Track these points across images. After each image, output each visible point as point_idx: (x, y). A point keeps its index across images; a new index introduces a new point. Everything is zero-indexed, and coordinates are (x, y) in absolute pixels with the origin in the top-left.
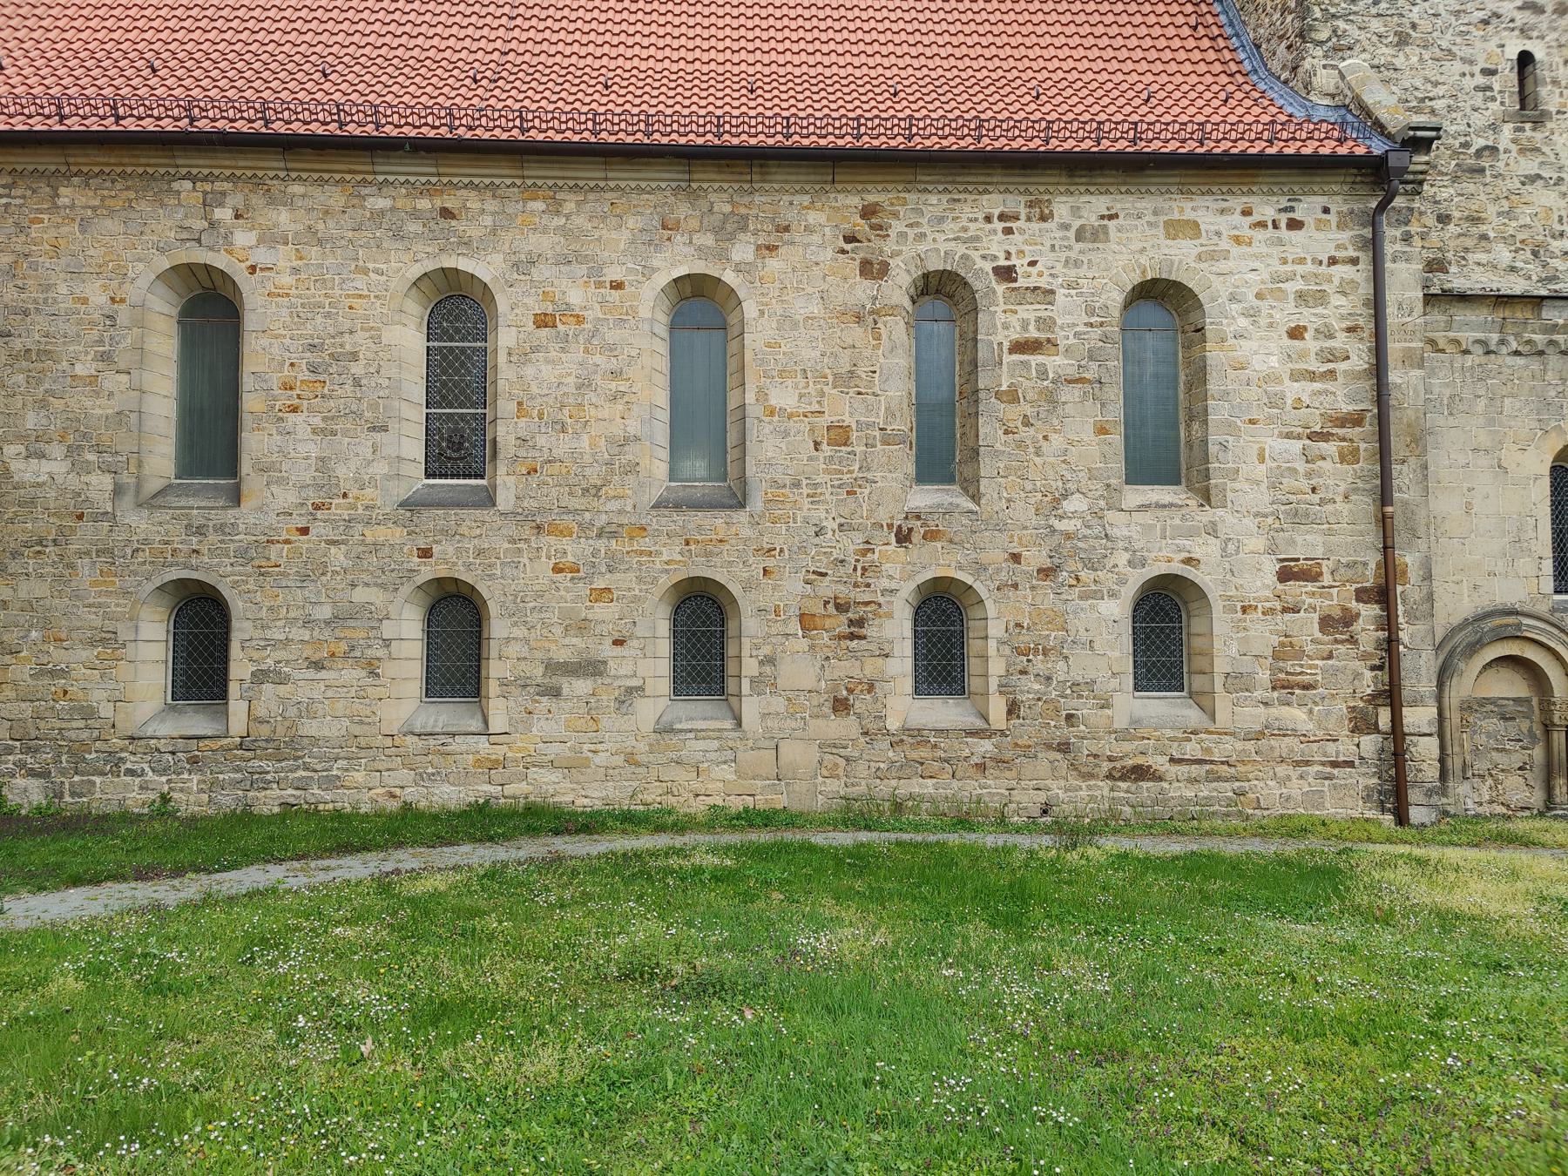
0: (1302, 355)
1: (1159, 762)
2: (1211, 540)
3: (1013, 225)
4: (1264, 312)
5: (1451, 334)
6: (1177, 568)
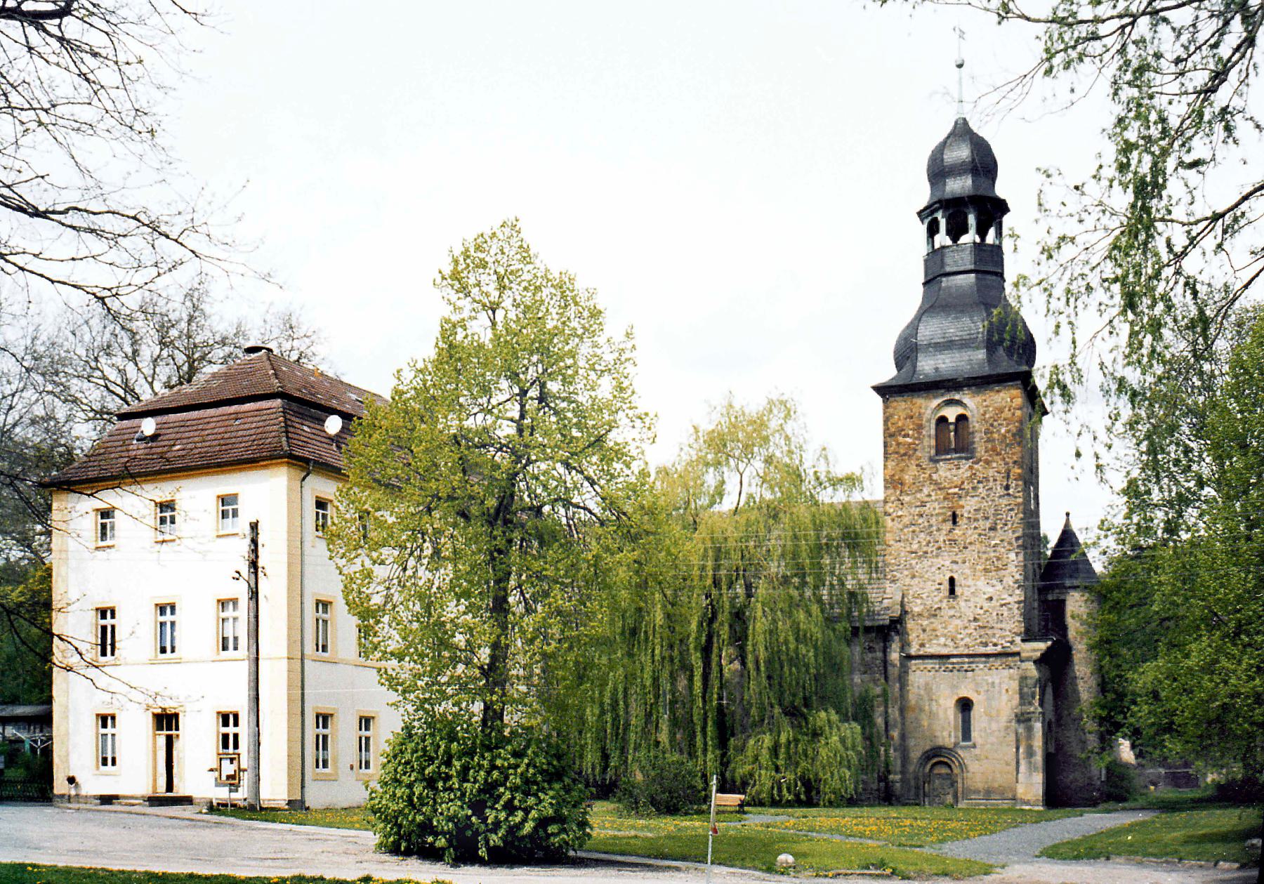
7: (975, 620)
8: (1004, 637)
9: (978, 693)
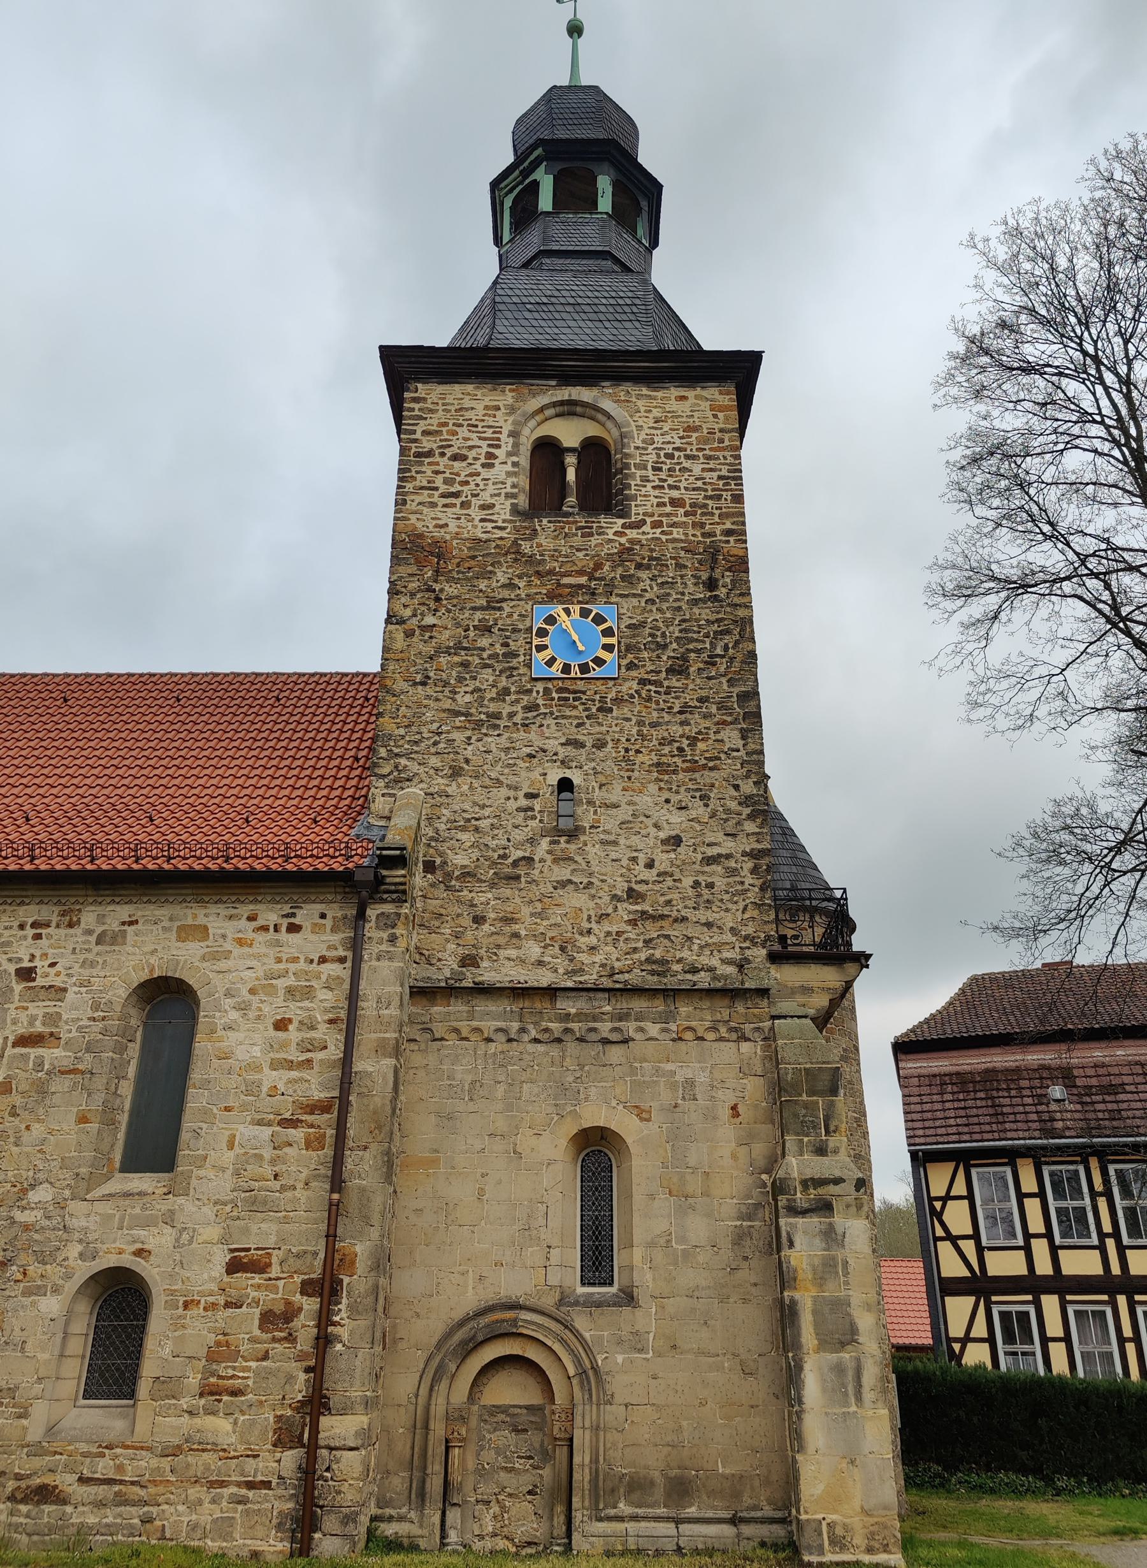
0: (284, 1045)
1: (66, 1482)
2: (167, 1230)
3: (43, 931)
4: (255, 1006)
5: (475, 1024)
6: (127, 1260)
7: (632, 895)
8: (719, 947)
9: (643, 1114)
